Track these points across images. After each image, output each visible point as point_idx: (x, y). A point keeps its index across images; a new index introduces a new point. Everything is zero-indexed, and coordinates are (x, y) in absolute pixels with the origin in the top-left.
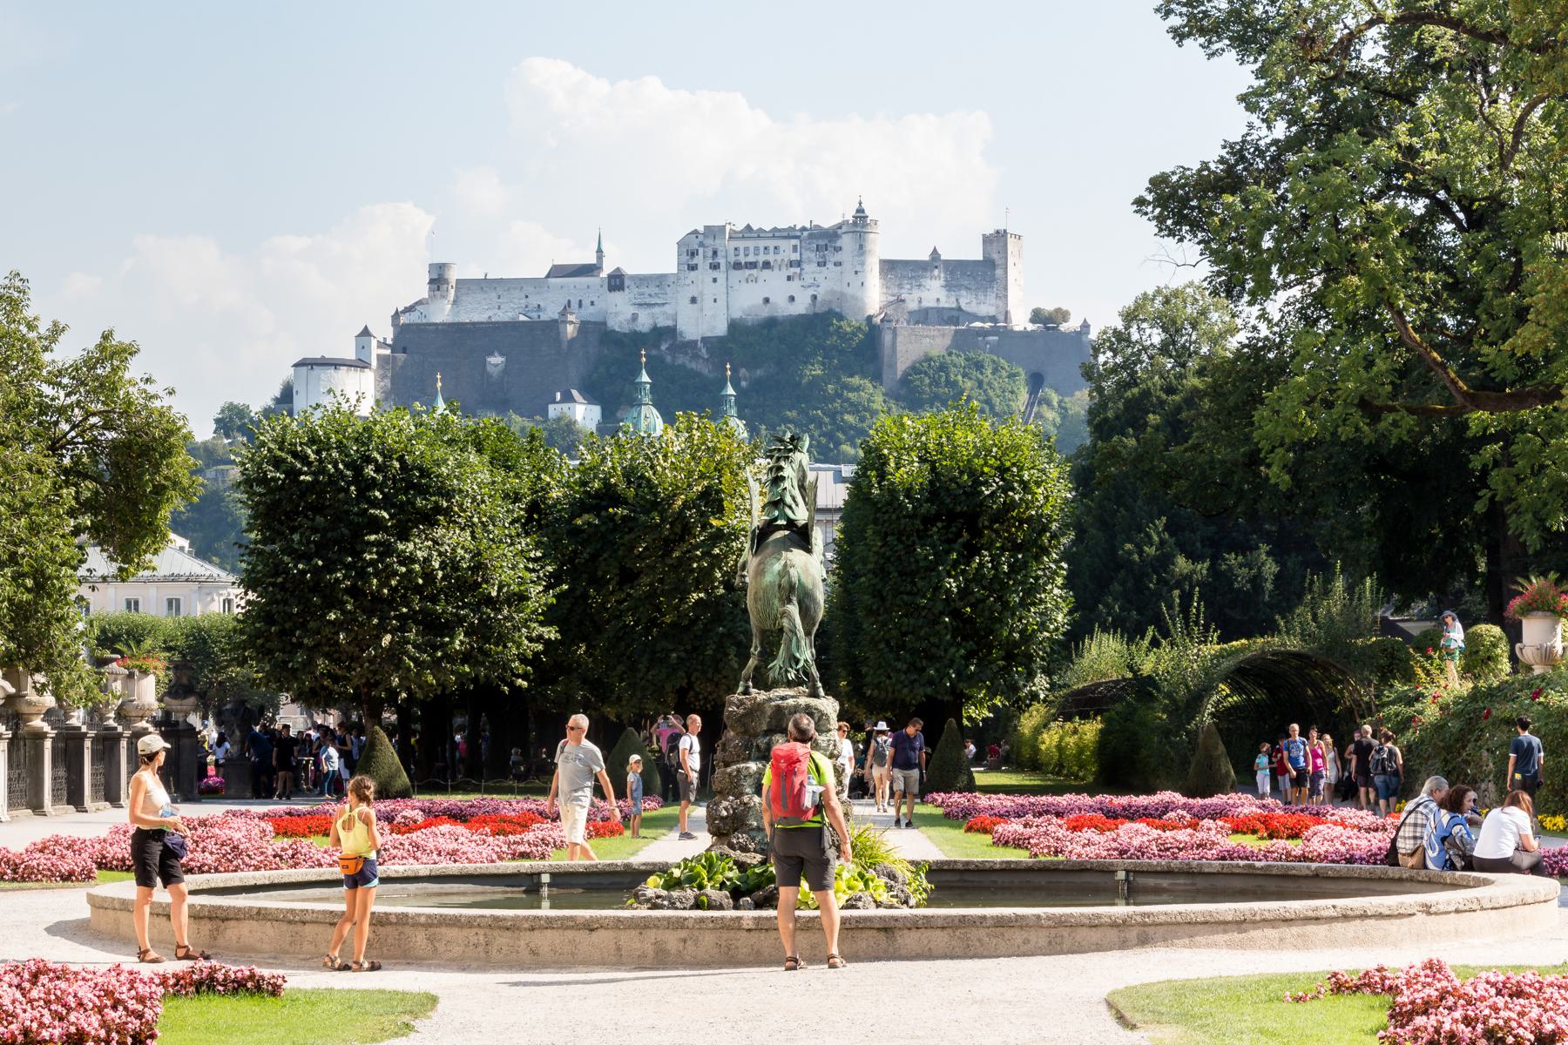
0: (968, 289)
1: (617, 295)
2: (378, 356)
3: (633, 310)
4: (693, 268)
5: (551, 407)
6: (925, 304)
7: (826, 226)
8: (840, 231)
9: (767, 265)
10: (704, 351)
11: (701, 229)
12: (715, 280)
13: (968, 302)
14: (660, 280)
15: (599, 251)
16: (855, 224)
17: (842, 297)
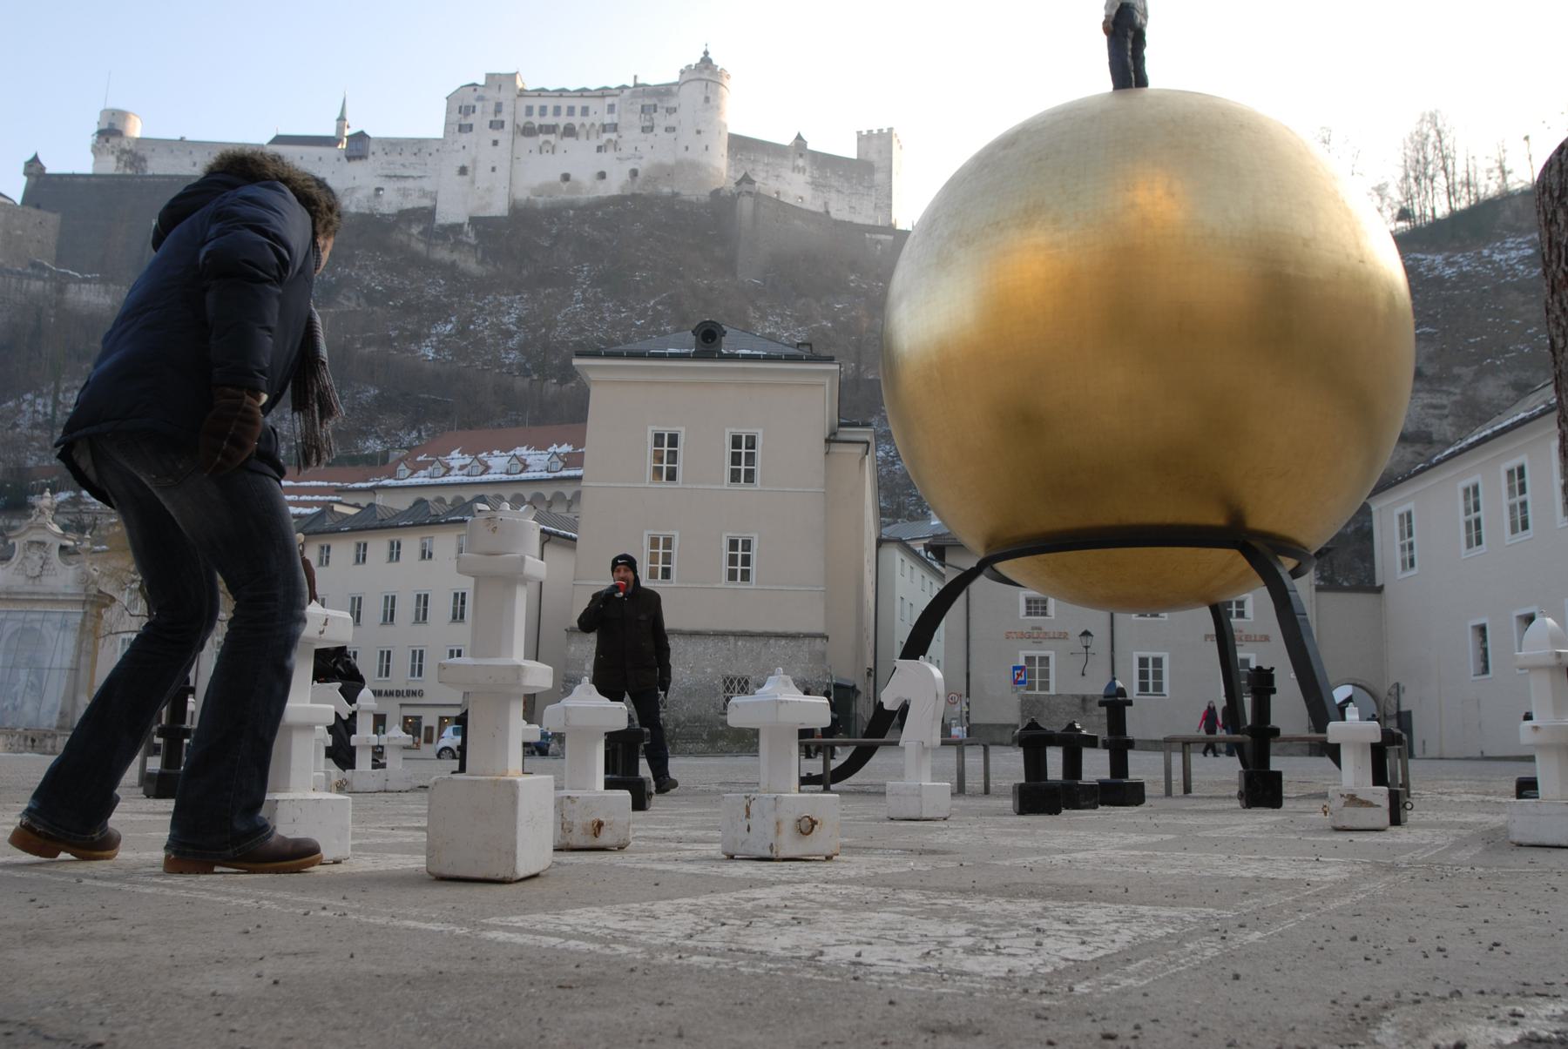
0: (839, 191)
1: (357, 166)
4: (465, 128)
9: (570, 131)
10: (471, 234)
11: (482, 81)
12: (495, 143)
13: (840, 210)
14: (418, 147)
15: (342, 119)
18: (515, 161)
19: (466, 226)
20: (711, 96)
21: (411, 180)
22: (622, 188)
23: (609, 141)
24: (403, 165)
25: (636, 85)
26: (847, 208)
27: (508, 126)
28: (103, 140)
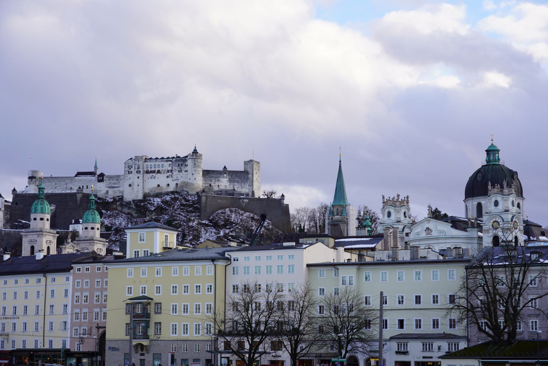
0: (238, 182)
1: (101, 184)
2: (5, 206)
3: (107, 189)
5: (71, 226)
6: (221, 188)
7: (182, 156)
8: (187, 158)
9: (159, 172)
10: (133, 205)
11: (134, 158)
12: (138, 177)
14: (118, 177)
15: (96, 167)
16: (193, 155)
17: (186, 184)
18: (144, 181)
19: (132, 202)
20: (196, 163)
21: (116, 188)
22: (174, 189)
23: (170, 175)
24: (114, 184)
25: (176, 158)
26: (240, 187)
27: (142, 173)
28: (31, 180)
